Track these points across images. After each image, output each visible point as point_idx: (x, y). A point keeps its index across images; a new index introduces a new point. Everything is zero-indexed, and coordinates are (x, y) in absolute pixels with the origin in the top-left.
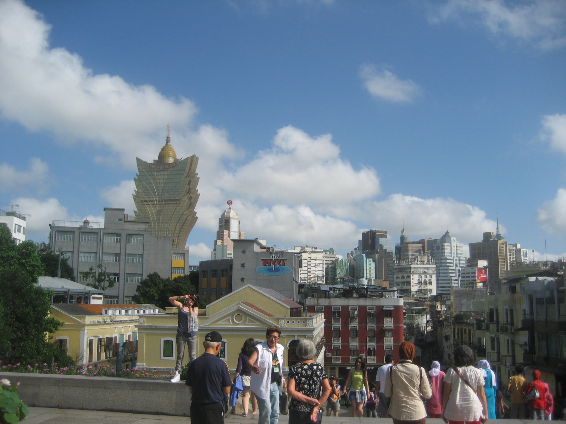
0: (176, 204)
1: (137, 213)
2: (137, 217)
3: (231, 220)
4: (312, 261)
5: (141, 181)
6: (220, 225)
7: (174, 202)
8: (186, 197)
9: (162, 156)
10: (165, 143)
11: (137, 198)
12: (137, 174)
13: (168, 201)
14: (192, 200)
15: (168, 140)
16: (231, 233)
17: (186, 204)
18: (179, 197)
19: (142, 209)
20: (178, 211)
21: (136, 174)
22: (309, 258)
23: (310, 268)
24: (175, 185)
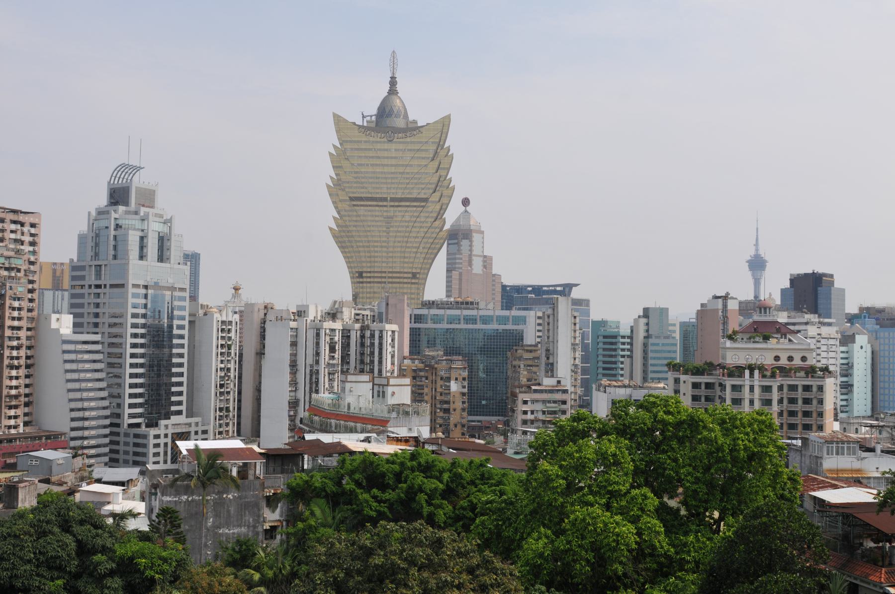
0: (419, 206)
1: (340, 221)
2: (340, 229)
3: (474, 234)
4: (823, 341)
5: (347, 159)
6: (450, 242)
7: (415, 204)
8: (438, 194)
9: (385, 111)
10: (387, 87)
11: (340, 193)
12: (335, 146)
13: (401, 200)
14: (444, 200)
15: (393, 82)
16: (474, 258)
17: (438, 207)
18: (425, 194)
19: (350, 213)
20: (423, 220)
21: (335, 146)
22: (819, 334)
23: (819, 355)
24: (416, 171)
